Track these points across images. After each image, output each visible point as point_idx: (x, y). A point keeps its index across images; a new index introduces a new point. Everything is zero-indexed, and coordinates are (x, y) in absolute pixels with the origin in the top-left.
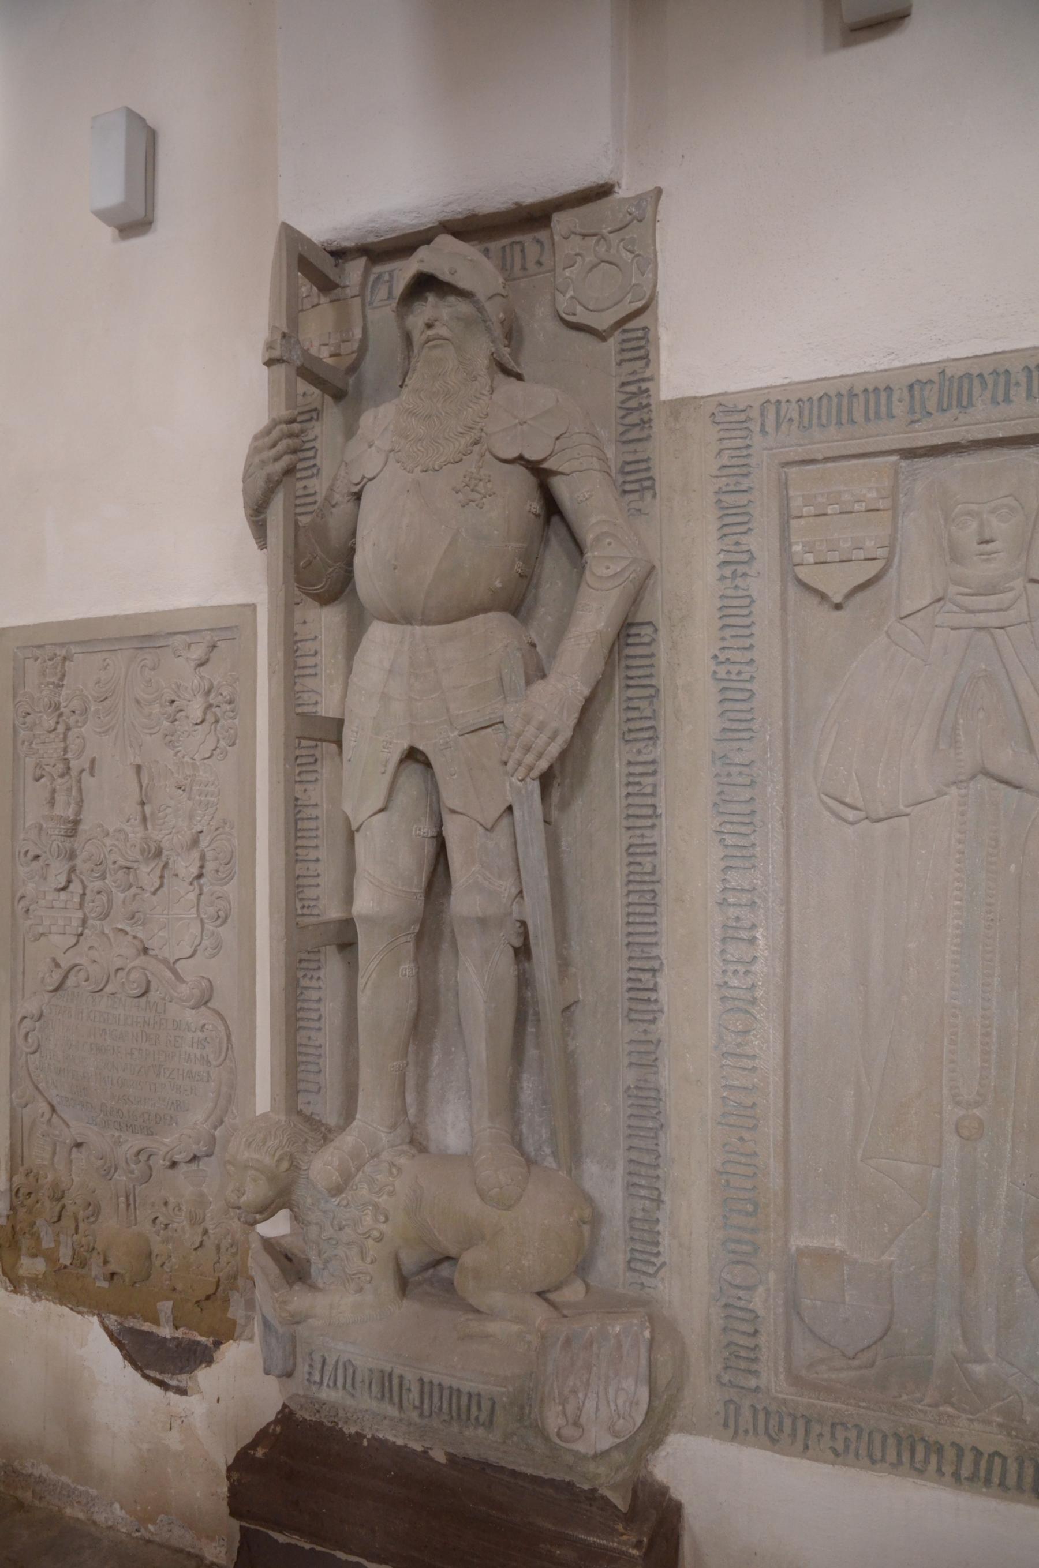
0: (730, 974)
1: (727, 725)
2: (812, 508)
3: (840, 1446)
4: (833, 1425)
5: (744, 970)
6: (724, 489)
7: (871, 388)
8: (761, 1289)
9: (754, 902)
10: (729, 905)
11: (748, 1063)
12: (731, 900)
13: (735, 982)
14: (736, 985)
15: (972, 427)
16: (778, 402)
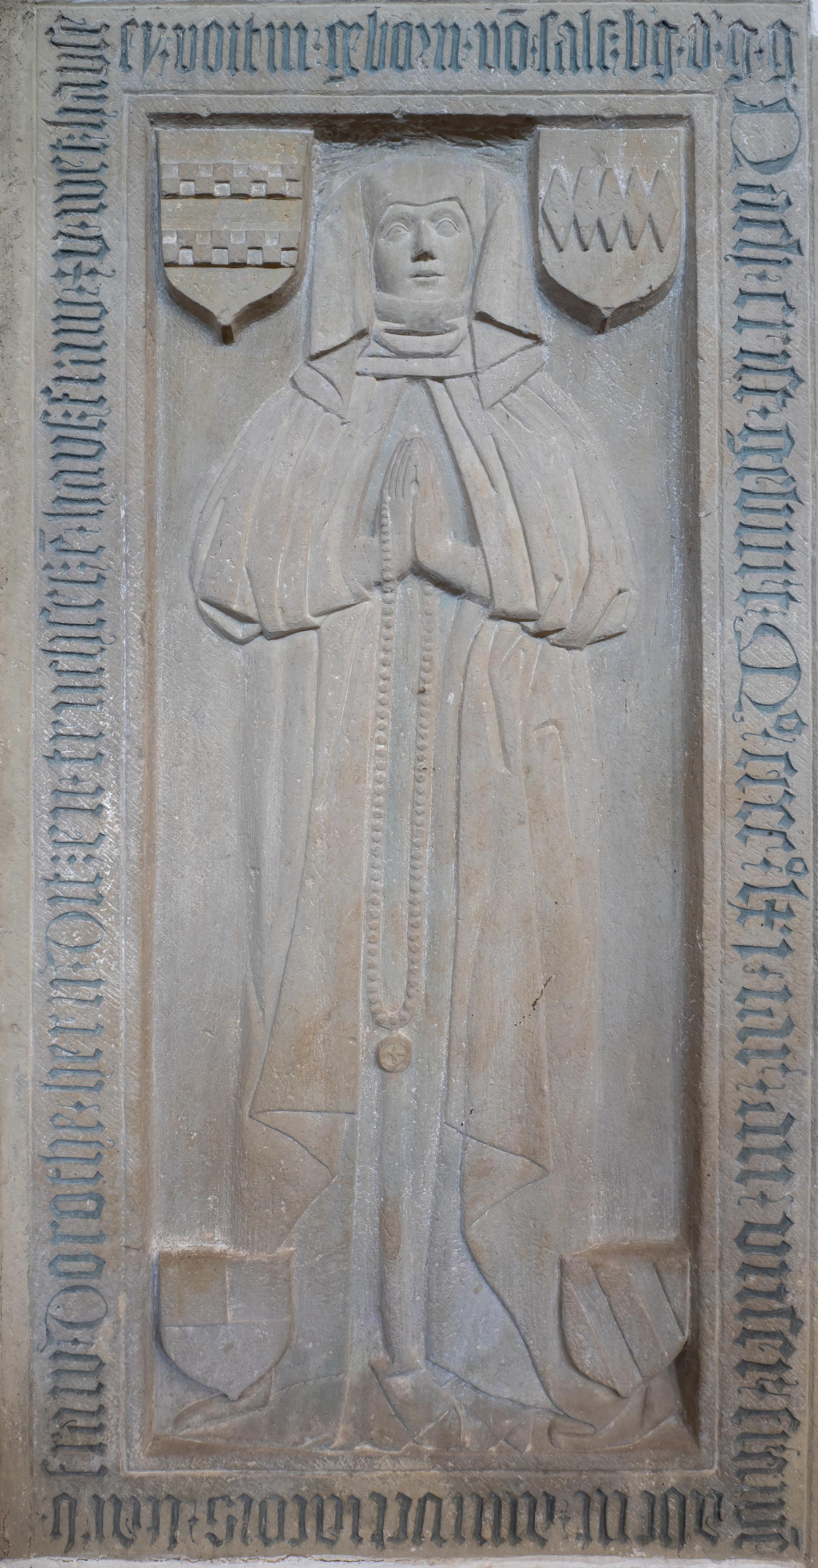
0: (63, 862)
1: (65, 492)
2: (192, 184)
3: (220, 1531)
4: (211, 1501)
5: (84, 855)
6: (66, 142)
7: (277, 24)
8: (107, 1323)
9: (100, 754)
10: (63, 759)
11: (90, 992)
12: (66, 753)
13: (70, 874)
14: (72, 877)
15: (409, 96)
16: (147, 25)
